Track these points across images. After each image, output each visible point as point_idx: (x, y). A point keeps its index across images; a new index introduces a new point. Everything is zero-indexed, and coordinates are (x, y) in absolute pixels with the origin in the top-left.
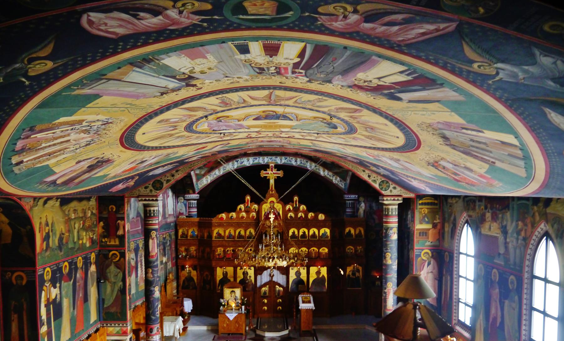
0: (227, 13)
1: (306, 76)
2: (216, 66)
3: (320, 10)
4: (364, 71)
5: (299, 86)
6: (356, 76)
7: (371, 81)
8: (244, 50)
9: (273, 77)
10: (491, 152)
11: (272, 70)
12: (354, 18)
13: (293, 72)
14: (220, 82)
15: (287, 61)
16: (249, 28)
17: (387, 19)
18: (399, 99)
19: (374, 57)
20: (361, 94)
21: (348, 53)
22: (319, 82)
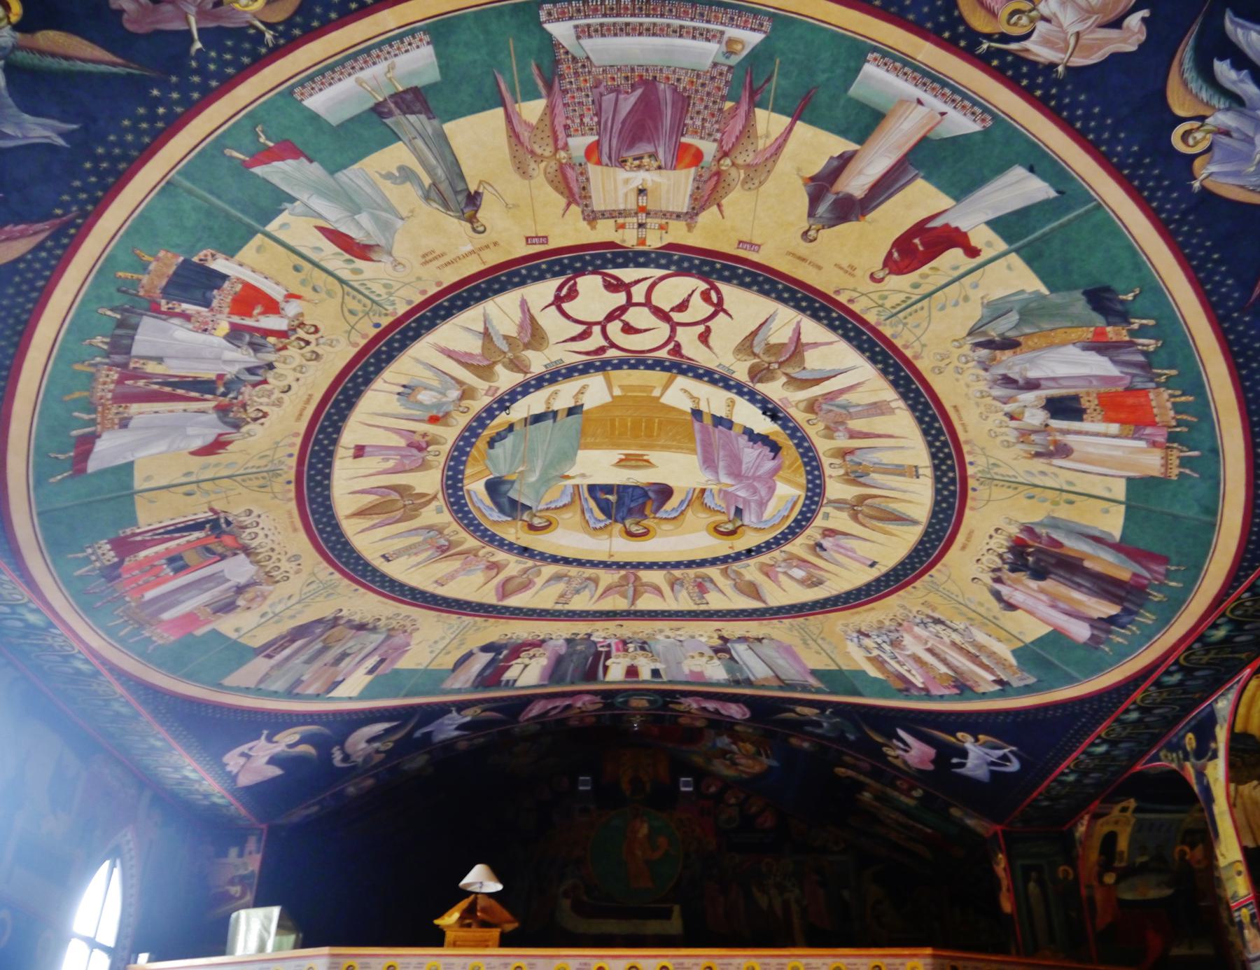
0: (660, 702)
1: (595, 643)
2: (686, 658)
3: (601, 705)
4: (544, 668)
5: (599, 625)
6: (549, 658)
7: (531, 658)
8: (656, 673)
9: (630, 635)
10: (309, 661)
11: (631, 647)
12: (579, 704)
13: (609, 646)
14: (690, 633)
15: (618, 661)
16: (648, 690)
17: (558, 710)
18: (485, 649)
19: (546, 683)
20: (525, 636)
21: (568, 679)
22: (579, 637)
